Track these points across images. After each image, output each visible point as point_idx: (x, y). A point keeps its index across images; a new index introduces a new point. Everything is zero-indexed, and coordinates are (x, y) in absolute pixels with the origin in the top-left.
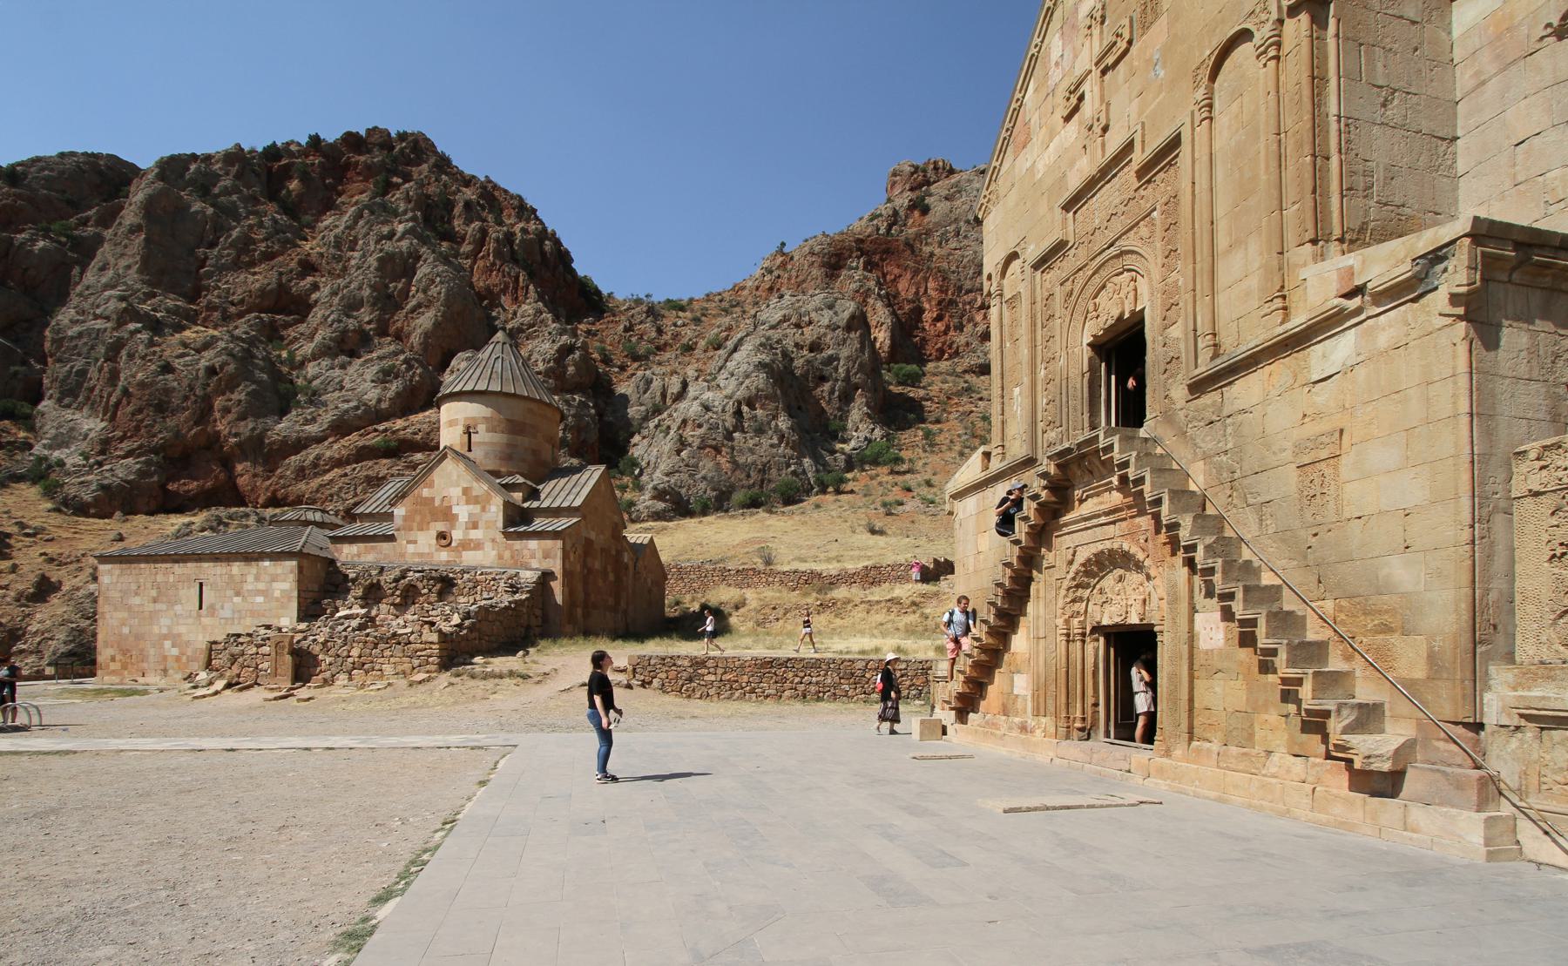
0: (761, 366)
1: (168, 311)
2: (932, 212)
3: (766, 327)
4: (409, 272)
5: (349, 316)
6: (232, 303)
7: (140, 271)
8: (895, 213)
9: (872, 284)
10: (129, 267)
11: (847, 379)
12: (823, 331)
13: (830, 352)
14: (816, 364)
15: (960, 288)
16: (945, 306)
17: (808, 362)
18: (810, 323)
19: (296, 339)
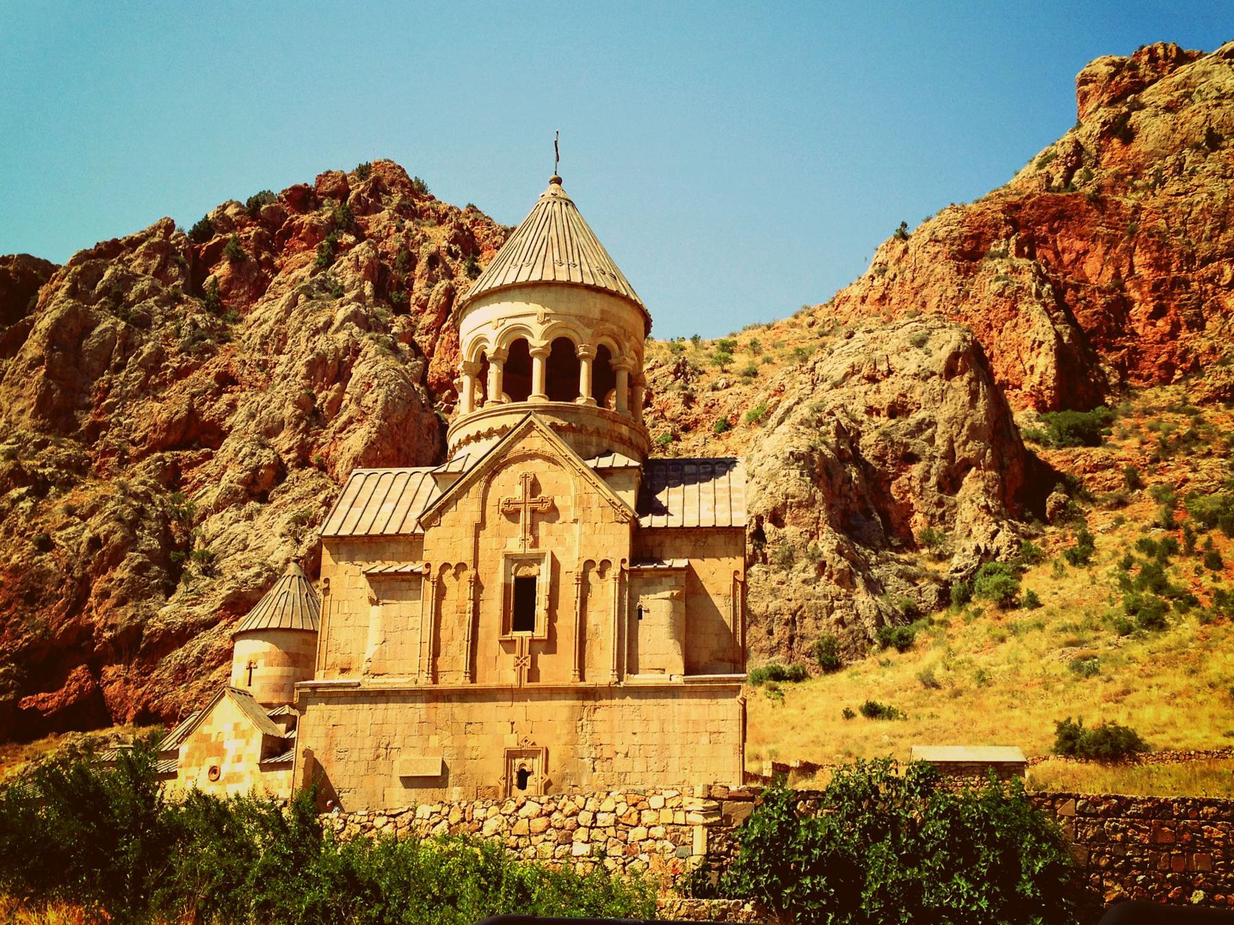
0: (796, 457)
1: (59, 465)
2: (1142, 134)
3: (826, 386)
4: (341, 373)
5: (264, 446)
6: (133, 443)
7: (34, 416)
8: (1078, 148)
9: (1027, 278)
10: (22, 412)
11: (950, 454)
12: (908, 382)
13: (921, 415)
14: (896, 437)
15: (1191, 258)
16: (1164, 292)
17: (885, 434)
18: (890, 372)
19: (201, 482)
